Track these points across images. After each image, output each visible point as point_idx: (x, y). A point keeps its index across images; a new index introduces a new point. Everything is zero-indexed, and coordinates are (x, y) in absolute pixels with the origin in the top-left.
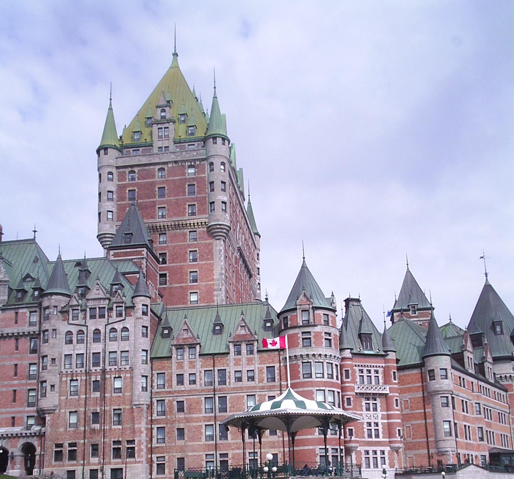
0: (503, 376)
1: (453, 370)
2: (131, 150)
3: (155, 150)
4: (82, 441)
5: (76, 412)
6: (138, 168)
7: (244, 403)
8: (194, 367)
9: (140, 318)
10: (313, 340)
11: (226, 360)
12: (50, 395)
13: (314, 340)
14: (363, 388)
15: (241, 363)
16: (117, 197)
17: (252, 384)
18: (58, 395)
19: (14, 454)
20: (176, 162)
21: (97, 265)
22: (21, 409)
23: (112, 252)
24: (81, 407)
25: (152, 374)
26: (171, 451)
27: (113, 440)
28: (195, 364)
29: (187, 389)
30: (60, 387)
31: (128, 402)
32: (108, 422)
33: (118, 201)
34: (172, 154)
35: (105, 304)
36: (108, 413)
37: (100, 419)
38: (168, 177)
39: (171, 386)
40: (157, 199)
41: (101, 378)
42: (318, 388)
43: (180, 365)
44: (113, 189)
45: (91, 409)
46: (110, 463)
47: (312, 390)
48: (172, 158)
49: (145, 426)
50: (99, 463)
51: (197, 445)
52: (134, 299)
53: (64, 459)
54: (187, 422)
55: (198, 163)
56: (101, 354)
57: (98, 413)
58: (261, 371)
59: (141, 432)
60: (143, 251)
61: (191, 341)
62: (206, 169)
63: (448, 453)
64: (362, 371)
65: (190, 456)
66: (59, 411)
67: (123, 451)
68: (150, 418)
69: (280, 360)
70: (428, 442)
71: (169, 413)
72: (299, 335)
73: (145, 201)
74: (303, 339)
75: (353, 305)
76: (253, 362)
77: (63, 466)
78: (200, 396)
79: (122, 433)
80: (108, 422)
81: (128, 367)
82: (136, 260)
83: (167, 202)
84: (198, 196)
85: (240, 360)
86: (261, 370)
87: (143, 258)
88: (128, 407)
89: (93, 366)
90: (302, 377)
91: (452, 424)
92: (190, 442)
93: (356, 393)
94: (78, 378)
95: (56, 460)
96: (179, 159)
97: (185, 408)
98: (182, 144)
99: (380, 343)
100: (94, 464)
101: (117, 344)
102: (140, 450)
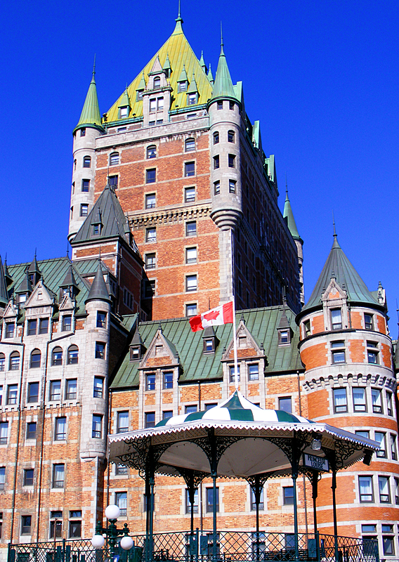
2: (116, 128)
3: (145, 124)
4: (10, 511)
6: (123, 149)
8: (170, 401)
9: (93, 331)
10: (348, 353)
11: (218, 390)
13: (350, 353)
20: (170, 136)
23: (74, 251)
26: (135, 529)
27: (51, 509)
33: (96, 191)
34: (165, 127)
35: (47, 313)
37: (35, 479)
40: (145, 184)
42: (358, 429)
43: (151, 400)
45: (24, 463)
48: (166, 132)
51: (173, 520)
55: (198, 134)
57: (33, 470)
59: (91, 499)
67: (65, 527)
72: (326, 347)
73: (130, 187)
74: (334, 352)
76: (258, 391)
82: (105, 258)
83: (159, 187)
84: (198, 176)
88: (74, 461)
89: (28, 402)
96: (174, 132)
98: (179, 115)
101: (62, 370)
102: (89, 525)
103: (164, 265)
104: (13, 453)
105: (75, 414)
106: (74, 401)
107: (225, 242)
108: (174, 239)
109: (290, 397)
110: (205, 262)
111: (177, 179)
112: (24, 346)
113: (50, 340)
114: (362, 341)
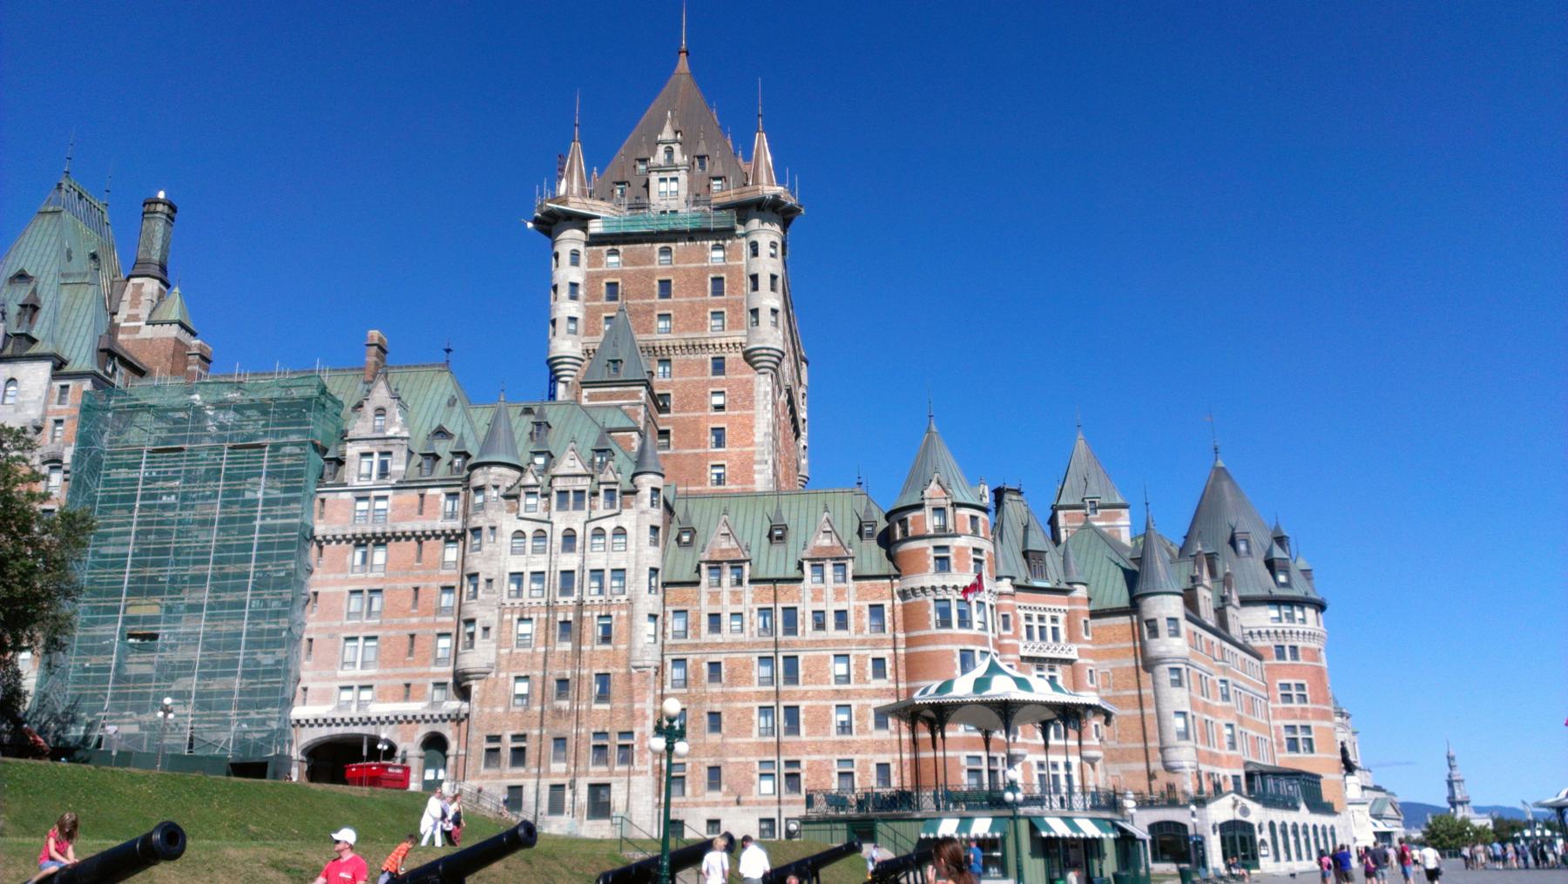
0: (1255, 631)
1: (1186, 622)
4: (536, 732)
5: (527, 677)
7: (829, 669)
8: (739, 601)
10: (953, 561)
12: (481, 646)
14: (1033, 648)
15: (824, 597)
16: (585, 293)
17: (842, 634)
18: (494, 645)
19: (409, 753)
21: (561, 413)
22: (423, 670)
23: (585, 392)
24: (537, 669)
25: (664, 612)
27: (593, 730)
28: (742, 596)
29: (727, 641)
30: (500, 631)
31: (622, 662)
32: (585, 697)
33: (587, 300)
35: (584, 484)
36: (586, 682)
37: (570, 692)
38: (677, 263)
39: (697, 635)
40: (656, 300)
41: (575, 618)
43: (715, 598)
44: (579, 279)
45: (556, 672)
46: (587, 774)
47: (952, 651)
49: (652, 705)
50: (567, 773)
52: (637, 478)
53: (502, 764)
54: (726, 701)
56: (576, 573)
58: (859, 612)
59: (646, 718)
60: (640, 391)
61: (734, 556)
62: (744, 253)
63: (1184, 770)
64: (1028, 618)
65: (732, 763)
66: (497, 676)
68: (659, 692)
69: (893, 595)
70: (1146, 751)
71: (693, 683)
75: (1011, 500)
76: (846, 596)
77: (501, 776)
78: (753, 654)
79: (611, 718)
80: (585, 697)
81: (623, 598)
82: (627, 407)
85: (821, 591)
86: (859, 611)
87: (640, 404)
88: (622, 670)
90: (933, 626)
91: (1190, 718)
92: (732, 737)
93: (1022, 658)
94: (532, 616)
95: (487, 765)
97: (723, 676)
99: (1060, 568)
100: (557, 775)
103: (682, 411)
104: (540, 660)
105: (624, 613)
106: (623, 598)
107: (762, 389)
108: (695, 378)
109: (882, 606)
110: (737, 413)
111: (699, 299)
112: (551, 523)
113: (587, 519)
114: (966, 548)
